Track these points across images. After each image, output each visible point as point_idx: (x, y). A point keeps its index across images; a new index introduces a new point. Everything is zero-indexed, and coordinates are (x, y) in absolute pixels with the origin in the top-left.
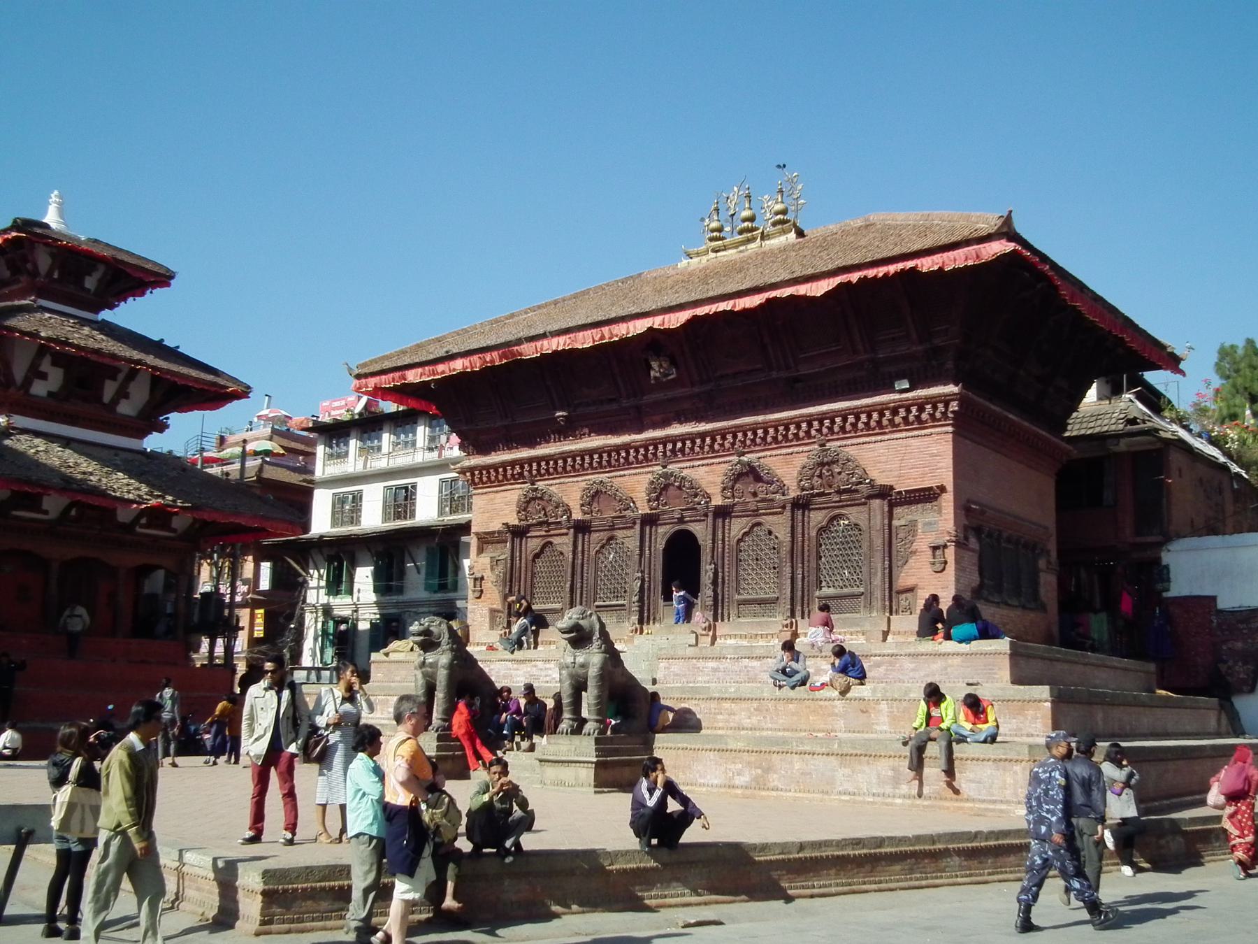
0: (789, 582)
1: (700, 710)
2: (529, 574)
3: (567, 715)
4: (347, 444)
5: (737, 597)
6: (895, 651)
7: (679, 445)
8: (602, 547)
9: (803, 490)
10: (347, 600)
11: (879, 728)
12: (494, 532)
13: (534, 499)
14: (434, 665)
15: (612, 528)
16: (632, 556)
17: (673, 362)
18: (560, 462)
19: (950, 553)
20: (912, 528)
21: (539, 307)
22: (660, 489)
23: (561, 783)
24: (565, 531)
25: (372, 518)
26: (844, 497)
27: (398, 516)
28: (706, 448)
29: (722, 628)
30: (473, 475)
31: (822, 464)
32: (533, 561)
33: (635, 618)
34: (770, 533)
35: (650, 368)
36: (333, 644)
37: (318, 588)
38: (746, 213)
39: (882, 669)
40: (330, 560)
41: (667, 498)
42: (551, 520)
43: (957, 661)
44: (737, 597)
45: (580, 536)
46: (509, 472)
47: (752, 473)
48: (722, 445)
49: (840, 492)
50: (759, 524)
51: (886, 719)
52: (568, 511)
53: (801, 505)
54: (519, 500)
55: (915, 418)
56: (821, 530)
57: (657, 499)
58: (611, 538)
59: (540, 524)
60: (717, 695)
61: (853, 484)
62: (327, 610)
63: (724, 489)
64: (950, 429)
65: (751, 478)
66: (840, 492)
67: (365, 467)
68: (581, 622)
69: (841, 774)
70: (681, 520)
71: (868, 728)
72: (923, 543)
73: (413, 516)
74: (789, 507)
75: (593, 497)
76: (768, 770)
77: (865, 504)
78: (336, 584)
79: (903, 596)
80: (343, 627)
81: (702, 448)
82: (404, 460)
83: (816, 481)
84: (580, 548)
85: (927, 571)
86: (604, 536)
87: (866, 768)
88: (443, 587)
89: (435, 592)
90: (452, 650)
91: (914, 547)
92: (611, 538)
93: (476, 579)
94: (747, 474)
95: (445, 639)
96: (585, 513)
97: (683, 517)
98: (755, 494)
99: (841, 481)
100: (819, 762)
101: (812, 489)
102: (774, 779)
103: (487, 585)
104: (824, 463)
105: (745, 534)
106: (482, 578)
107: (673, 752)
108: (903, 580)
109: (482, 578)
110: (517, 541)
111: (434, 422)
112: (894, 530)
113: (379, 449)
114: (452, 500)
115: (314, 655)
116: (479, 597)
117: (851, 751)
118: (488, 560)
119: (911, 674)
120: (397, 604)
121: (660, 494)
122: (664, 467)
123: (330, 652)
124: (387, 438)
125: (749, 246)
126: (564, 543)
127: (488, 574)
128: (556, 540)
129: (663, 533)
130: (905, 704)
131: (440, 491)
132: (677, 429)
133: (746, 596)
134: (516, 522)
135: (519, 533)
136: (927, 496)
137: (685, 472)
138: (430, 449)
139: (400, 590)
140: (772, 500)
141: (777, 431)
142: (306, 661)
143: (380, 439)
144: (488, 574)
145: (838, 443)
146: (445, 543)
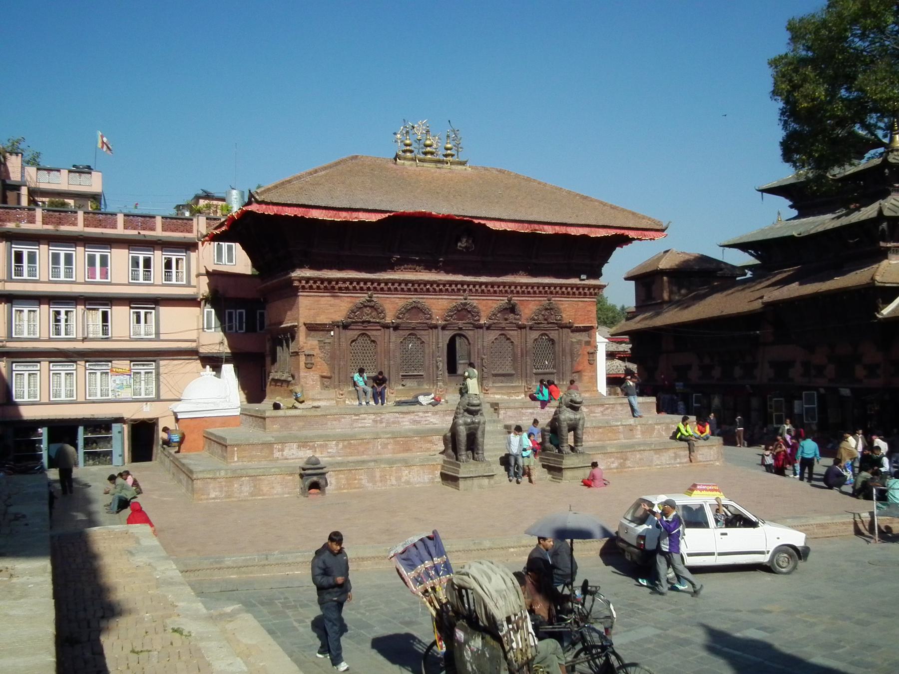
15: (414, 329)
31: (547, 309)
35: (459, 240)
39: (609, 410)
42: (372, 320)
59: (363, 322)
69: (655, 457)
70: (460, 329)
71: (633, 437)
76: (626, 460)
83: (541, 317)
85: (586, 363)
100: (646, 454)
102: (628, 463)
104: (549, 309)
118: (316, 342)
127: (316, 352)
132: (483, 279)
135: (346, 327)
144: (316, 352)
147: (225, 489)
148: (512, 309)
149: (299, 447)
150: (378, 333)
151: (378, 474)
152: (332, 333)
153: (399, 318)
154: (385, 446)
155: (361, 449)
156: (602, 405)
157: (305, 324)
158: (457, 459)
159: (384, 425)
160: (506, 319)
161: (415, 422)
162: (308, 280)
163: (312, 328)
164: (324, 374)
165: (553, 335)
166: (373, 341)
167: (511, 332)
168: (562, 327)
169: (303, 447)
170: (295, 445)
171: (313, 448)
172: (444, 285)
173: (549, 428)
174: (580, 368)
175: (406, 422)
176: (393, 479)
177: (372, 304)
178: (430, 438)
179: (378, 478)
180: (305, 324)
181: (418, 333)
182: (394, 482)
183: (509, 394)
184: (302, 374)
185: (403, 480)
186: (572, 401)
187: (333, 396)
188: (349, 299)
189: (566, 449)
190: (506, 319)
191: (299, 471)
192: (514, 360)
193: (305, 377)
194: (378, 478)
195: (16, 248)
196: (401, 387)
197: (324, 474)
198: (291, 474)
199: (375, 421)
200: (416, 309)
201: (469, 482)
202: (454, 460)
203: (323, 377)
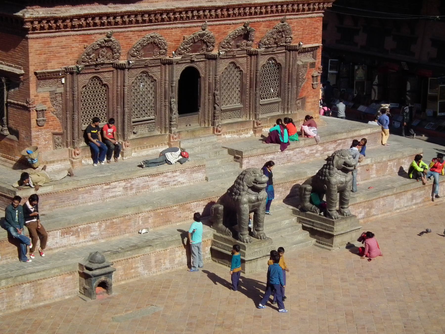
11: (372, 176)
15: (146, 66)
70: (192, 61)
71: (368, 177)
76: (371, 208)
83: (272, 41)
85: (310, 88)
100: (389, 199)
102: (373, 211)
104: (282, 32)
130: (381, 164)
147: (6, 300)
148: (246, 35)
149: (63, 234)
151: (153, 259)
152: (63, 80)
154: (146, 220)
155: (123, 227)
156: (335, 141)
157: (36, 74)
158: (236, 236)
159: (134, 191)
161: (164, 184)
162: (40, 20)
163: (42, 77)
164: (57, 131)
165: (281, 58)
166: (105, 85)
167: (240, 60)
168: (290, 49)
169: (67, 233)
170: (59, 233)
171: (77, 233)
172: (180, 13)
173: (309, 187)
174: (304, 94)
175: (155, 185)
176: (167, 262)
177: (110, 44)
178: (188, 206)
179: (153, 264)
180: (36, 74)
182: (168, 265)
183: (237, 132)
184: (34, 134)
185: (176, 262)
186: (345, 164)
187: (67, 155)
188: (81, 38)
189: (335, 213)
190: (238, 46)
191: (78, 269)
192: (242, 92)
193: (37, 137)
194: (153, 264)
196: (132, 136)
197: (110, 273)
198: (71, 273)
199: (125, 188)
200: (154, 44)
201: (254, 263)
202: (231, 238)
203: (54, 134)
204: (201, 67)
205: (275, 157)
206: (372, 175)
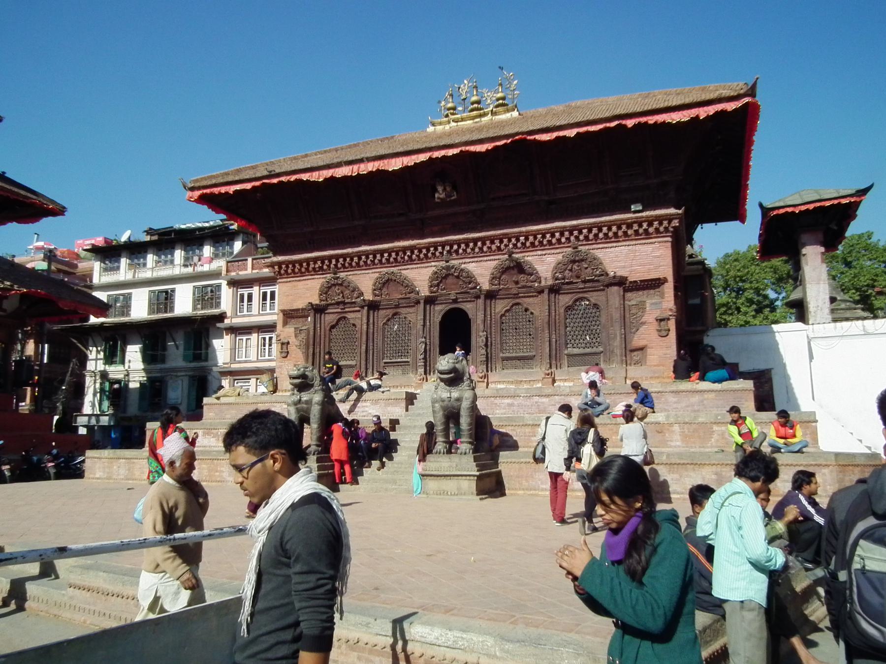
0: (548, 343)
1: (516, 434)
2: (327, 339)
3: (440, 439)
4: (119, 262)
5: (501, 355)
6: (660, 389)
7: (455, 247)
8: (388, 320)
9: (556, 279)
10: (120, 368)
11: (673, 444)
12: (298, 310)
13: (334, 285)
14: (309, 402)
15: (397, 307)
16: (421, 325)
17: (455, 188)
18: (356, 259)
19: (672, 324)
20: (641, 306)
21: (325, 152)
22: (439, 279)
23: (445, 493)
24: (358, 309)
25: (140, 309)
26: (587, 285)
27: (159, 311)
28: (477, 250)
29: (493, 377)
30: (280, 268)
31: (574, 262)
32: (330, 330)
33: (421, 371)
34: (526, 310)
35: (436, 191)
36: (108, 398)
37: (96, 359)
38: (474, 98)
40: (106, 340)
41: (446, 284)
42: (347, 301)
43: (712, 395)
44: (501, 355)
45: (371, 312)
46: (312, 266)
47: (519, 268)
48: (489, 248)
49: (585, 282)
50: (518, 304)
51: (679, 437)
52: (362, 294)
53: (554, 290)
54: (322, 286)
55: (641, 232)
56: (568, 308)
57: (438, 285)
58: (395, 314)
59: (338, 303)
60: (531, 423)
61: (596, 276)
62: (104, 375)
63: (493, 278)
64: (669, 239)
65: (516, 271)
66: (585, 282)
67: (134, 277)
68: (457, 366)
70: (455, 301)
72: (650, 316)
73: (172, 310)
74: (546, 291)
75: (384, 284)
77: (603, 290)
78: (113, 356)
79: (635, 353)
80: (116, 386)
81: (473, 249)
82: (165, 272)
84: (371, 321)
86: (390, 312)
87: (692, 474)
88: (197, 358)
89: (190, 362)
90: (323, 390)
91: (643, 320)
92: (395, 314)
93: (283, 344)
94: (513, 268)
95: (317, 382)
96: (376, 295)
97: (457, 299)
98: (517, 283)
99: (587, 274)
101: (564, 279)
103: (292, 348)
104: (576, 260)
105: (507, 311)
106: (288, 343)
107: (517, 466)
108: (637, 341)
109: (288, 343)
110: (318, 316)
111: (188, 248)
112: (627, 308)
113: (145, 265)
114: (203, 300)
115: (93, 406)
116: (286, 357)
117: (679, 462)
119: (675, 406)
120: (161, 370)
121: (441, 282)
122: (447, 262)
123: (106, 404)
124: (151, 258)
125: (483, 119)
126: (358, 318)
127: (292, 340)
128: (349, 316)
129: (439, 310)
130: (694, 426)
131: (194, 294)
133: (507, 355)
134: (317, 302)
135: (318, 310)
136: (655, 284)
137: (463, 266)
138: (185, 266)
139: (163, 360)
140: (531, 287)
141: (535, 238)
142: (87, 409)
143: (145, 258)
144: (292, 340)
145: (587, 247)
146: (200, 330)
150: (358, 315)
153: (376, 295)
160: (517, 283)
166: (354, 325)
181: (403, 311)
195: (241, 291)
204: (468, 307)
205: (516, 403)
206: (671, 441)
